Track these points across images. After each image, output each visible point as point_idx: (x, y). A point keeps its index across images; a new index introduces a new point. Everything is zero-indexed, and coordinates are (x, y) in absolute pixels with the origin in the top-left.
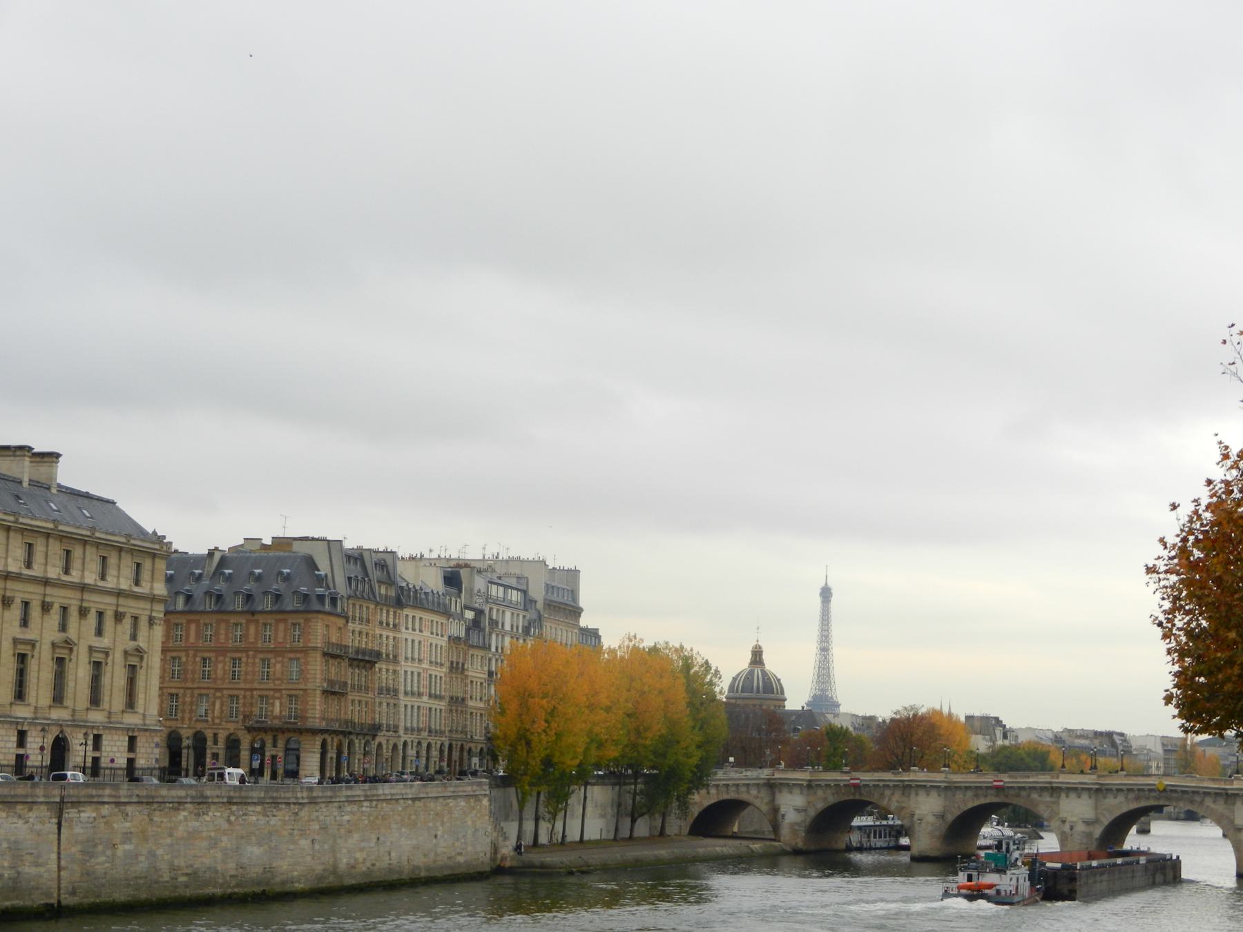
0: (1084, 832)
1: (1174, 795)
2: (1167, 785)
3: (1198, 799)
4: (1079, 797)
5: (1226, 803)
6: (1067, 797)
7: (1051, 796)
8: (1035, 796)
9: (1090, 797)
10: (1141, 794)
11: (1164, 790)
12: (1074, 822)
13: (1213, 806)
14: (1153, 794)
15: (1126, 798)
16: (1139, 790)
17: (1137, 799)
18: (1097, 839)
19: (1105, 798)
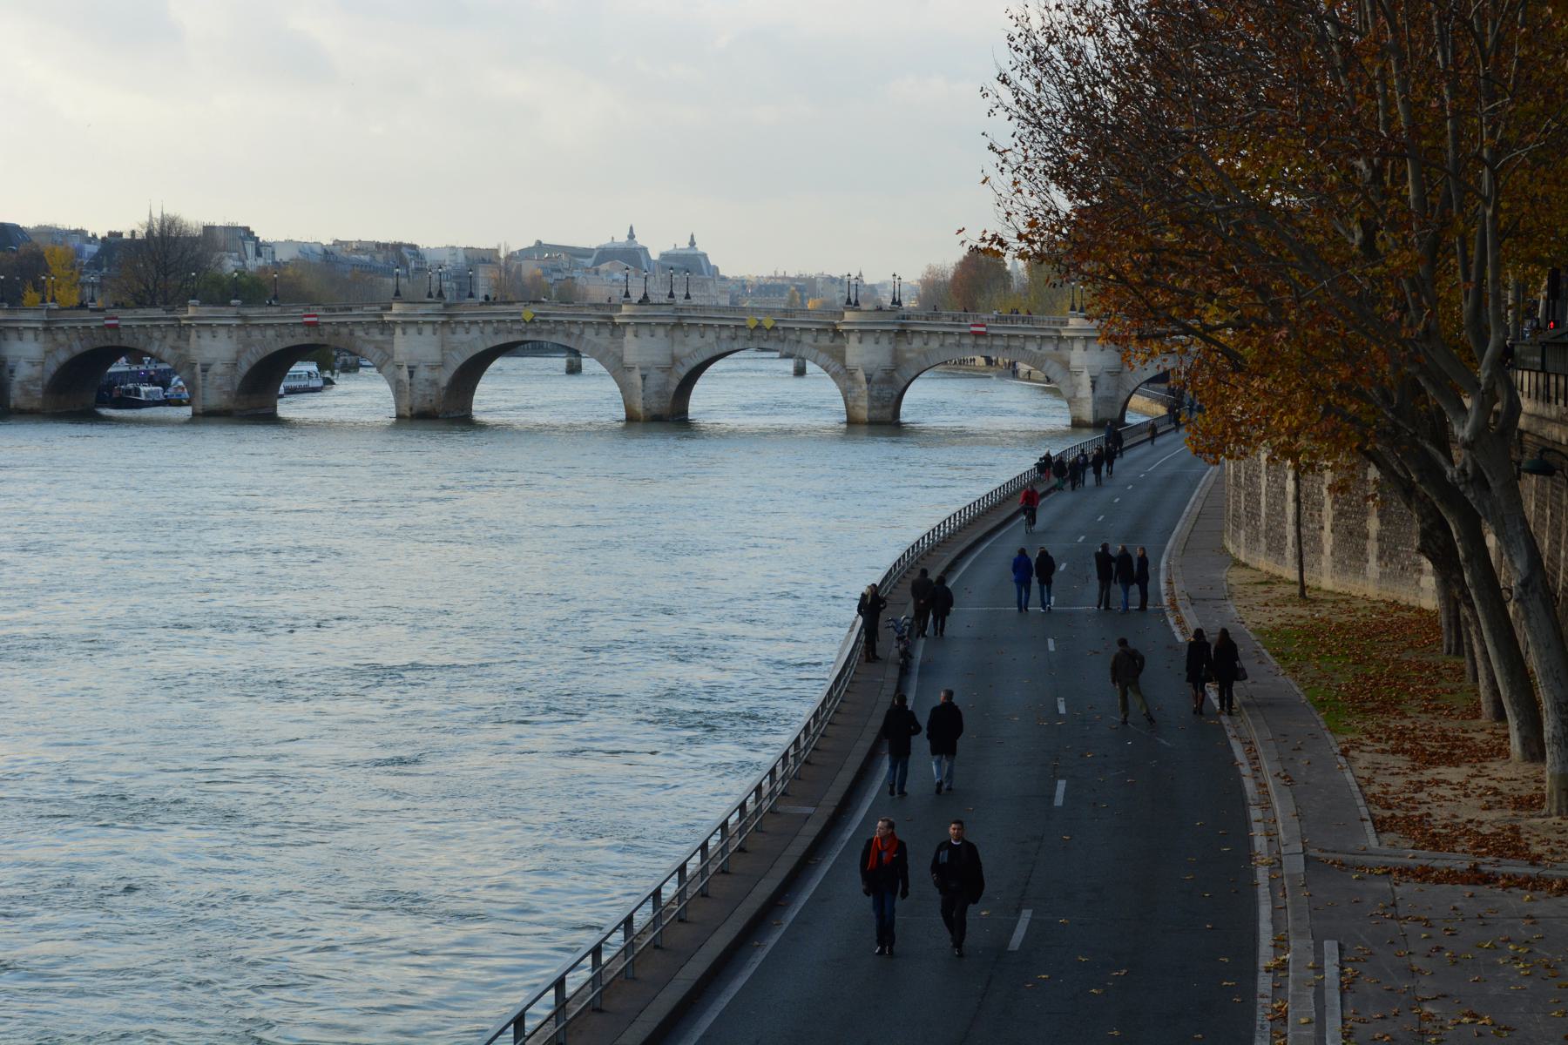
0: (427, 380)
1: (545, 327)
2: (536, 314)
3: (575, 330)
4: (420, 334)
5: (612, 335)
6: (404, 333)
7: (382, 334)
8: (359, 333)
9: (435, 334)
10: (502, 326)
11: (532, 321)
12: (414, 367)
13: (595, 340)
14: (516, 327)
15: (482, 333)
16: (498, 321)
17: (497, 332)
18: (443, 389)
19: (454, 333)
